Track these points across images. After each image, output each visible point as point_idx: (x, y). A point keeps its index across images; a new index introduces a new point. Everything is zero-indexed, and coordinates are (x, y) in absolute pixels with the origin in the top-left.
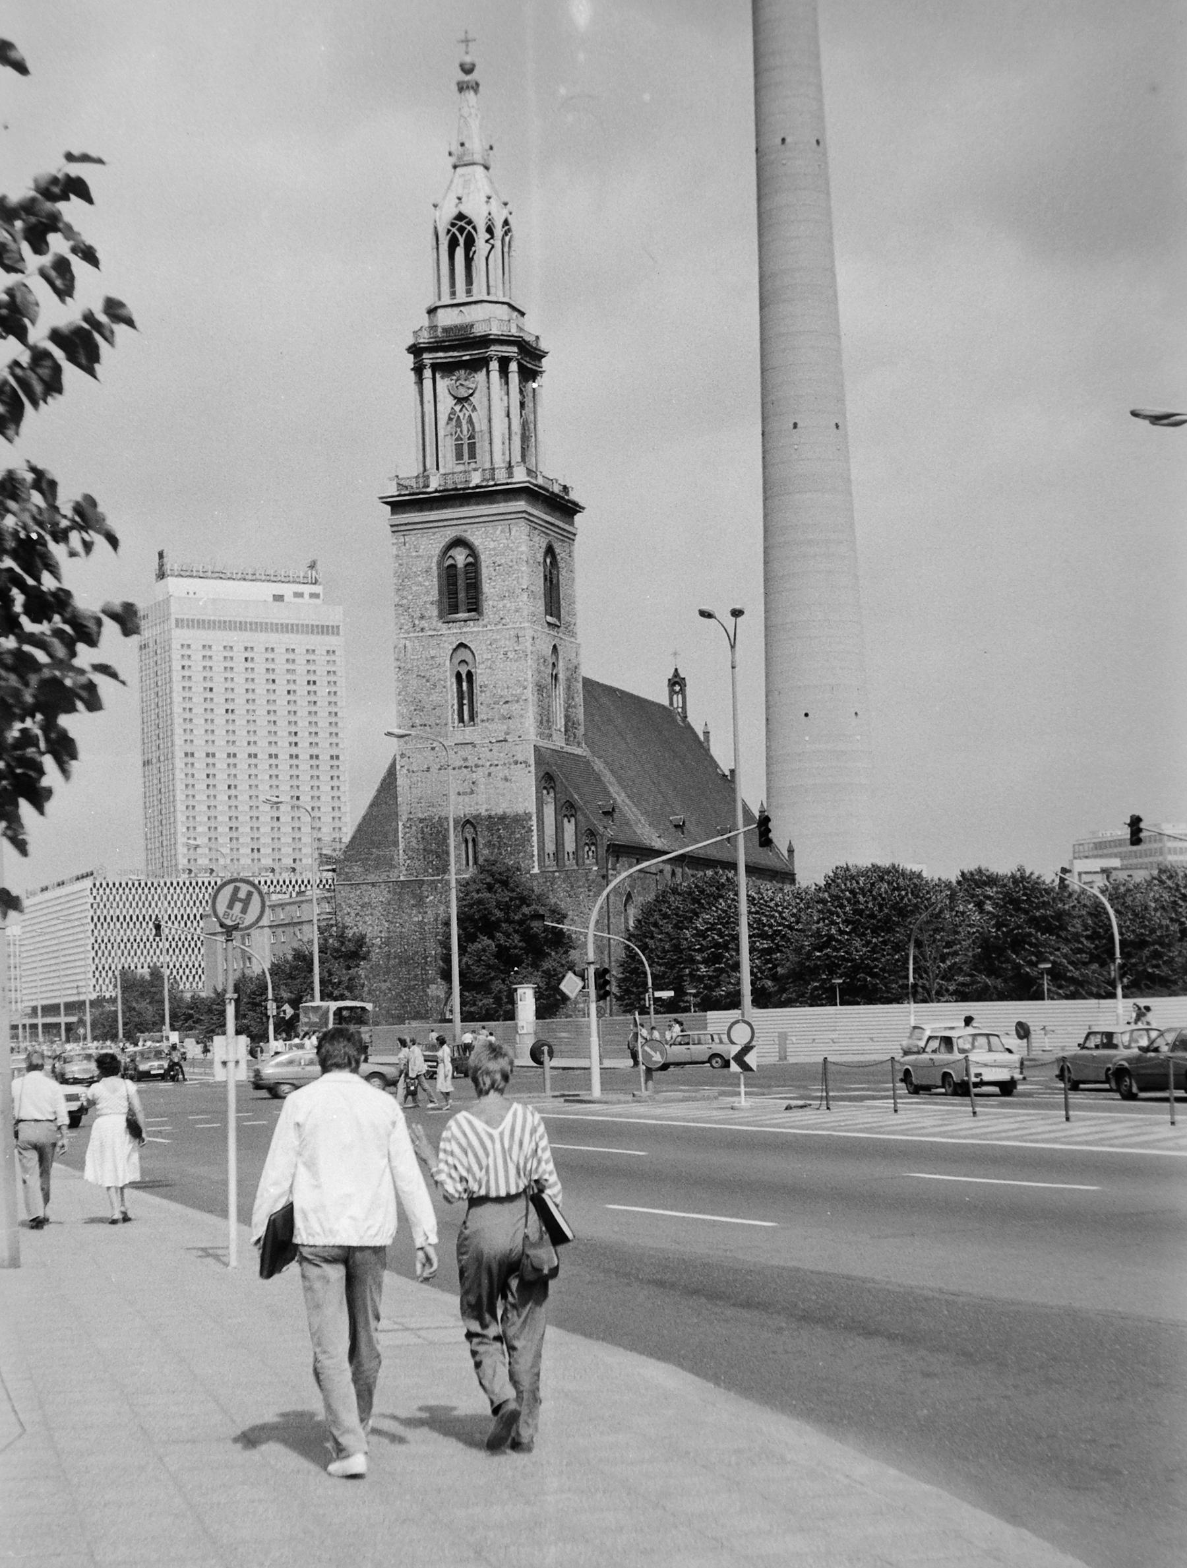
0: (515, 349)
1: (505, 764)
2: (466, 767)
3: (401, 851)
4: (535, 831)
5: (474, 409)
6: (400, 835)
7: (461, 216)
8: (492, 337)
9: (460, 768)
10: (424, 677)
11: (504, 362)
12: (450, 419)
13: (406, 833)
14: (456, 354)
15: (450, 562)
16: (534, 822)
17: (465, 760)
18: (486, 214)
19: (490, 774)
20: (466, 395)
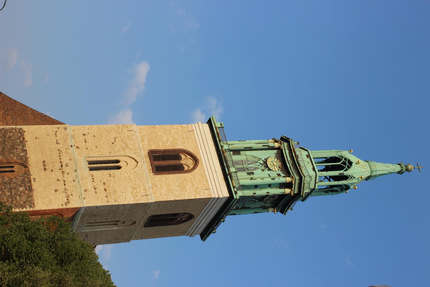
0: (296, 192)
1: (66, 190)
2: (62, 166)
3: (3, 127)
4: (22, 210)
5: (263, 170)
6: (14, 127)
7: (350, 163)
8: (303, 178)
9: (61, 162)
10: (115, 141)
11: (288, 185)
12: (255, 157)
13: (16, 130)
14: (289, 159)
15: (183, 156)
16: (28, 209)
17: (67, 165)
18: (354, 176)
19: (58, 180)
20: (269, 165)
